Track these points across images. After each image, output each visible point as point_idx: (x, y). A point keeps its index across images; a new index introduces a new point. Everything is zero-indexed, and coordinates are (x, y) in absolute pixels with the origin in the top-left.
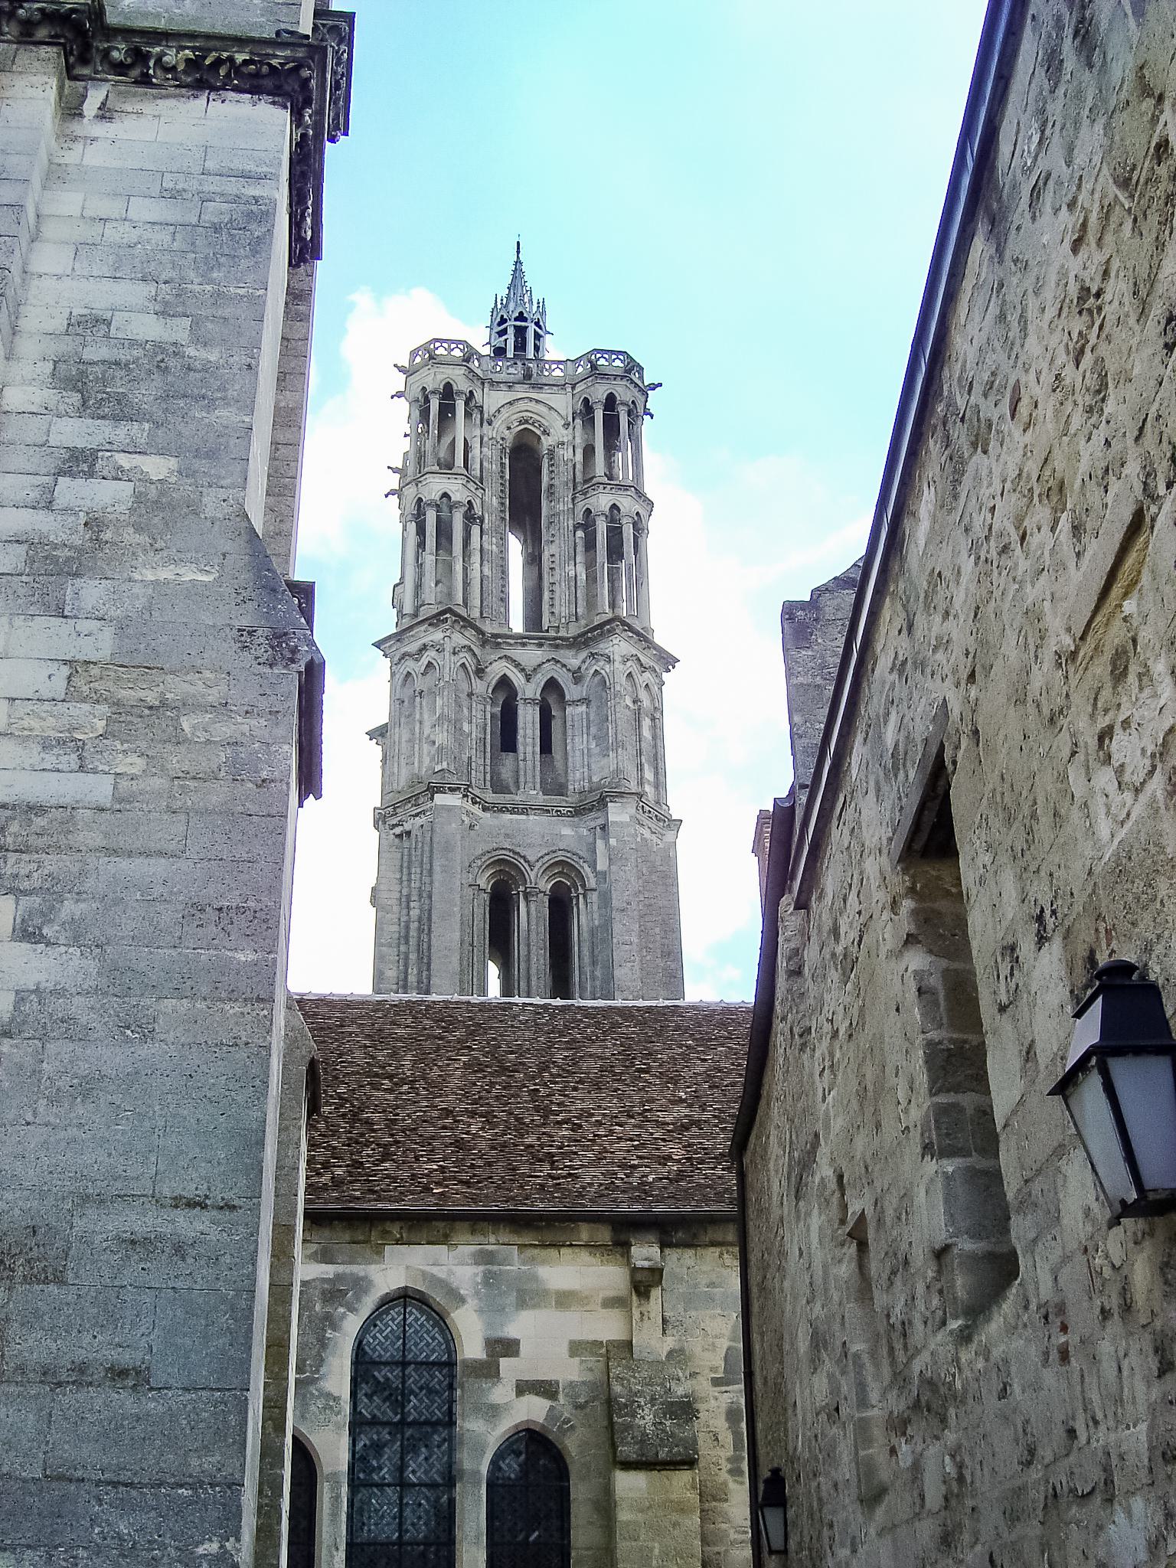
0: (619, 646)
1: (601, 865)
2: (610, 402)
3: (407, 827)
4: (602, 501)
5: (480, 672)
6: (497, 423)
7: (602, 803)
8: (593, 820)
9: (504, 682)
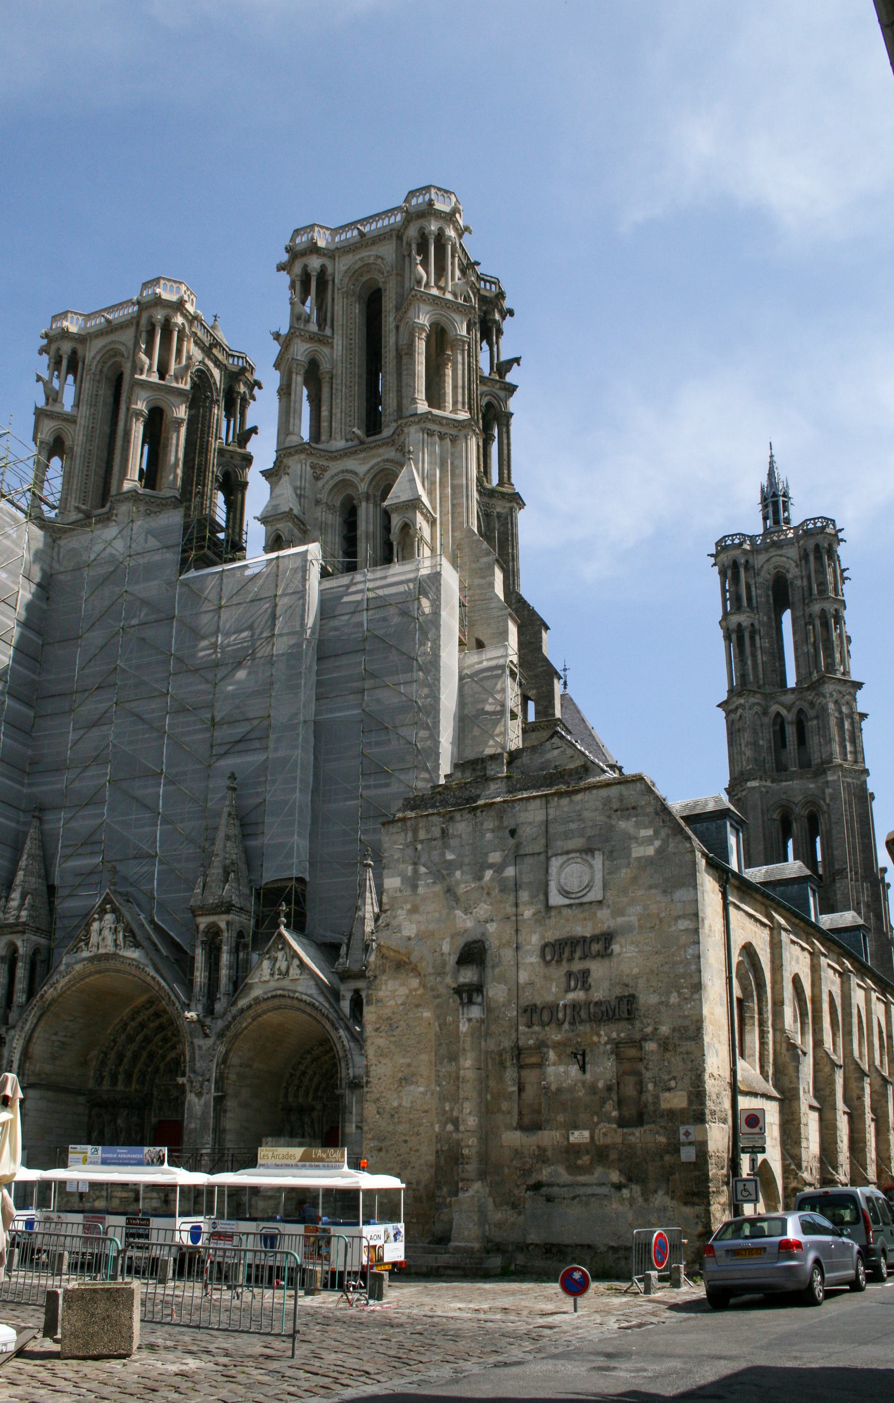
0: (829, 688)
1: (828, 801)
2: (817, 547)
3: (739, 796)
4: (816, 608)
5: (765, 713)
6: (763, 573)
7: (824, 772)
8: (821, 780)
9: (778, 714)
